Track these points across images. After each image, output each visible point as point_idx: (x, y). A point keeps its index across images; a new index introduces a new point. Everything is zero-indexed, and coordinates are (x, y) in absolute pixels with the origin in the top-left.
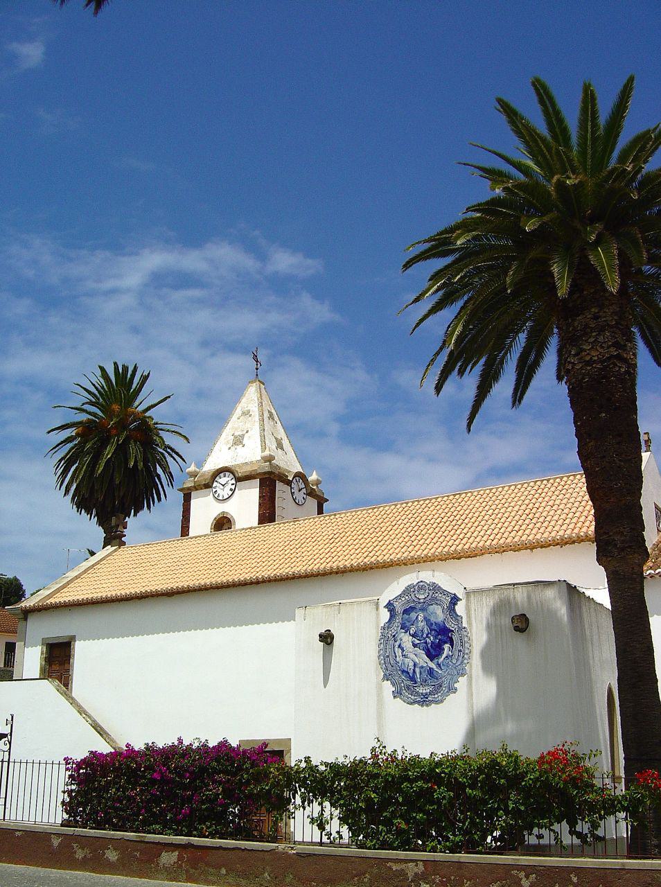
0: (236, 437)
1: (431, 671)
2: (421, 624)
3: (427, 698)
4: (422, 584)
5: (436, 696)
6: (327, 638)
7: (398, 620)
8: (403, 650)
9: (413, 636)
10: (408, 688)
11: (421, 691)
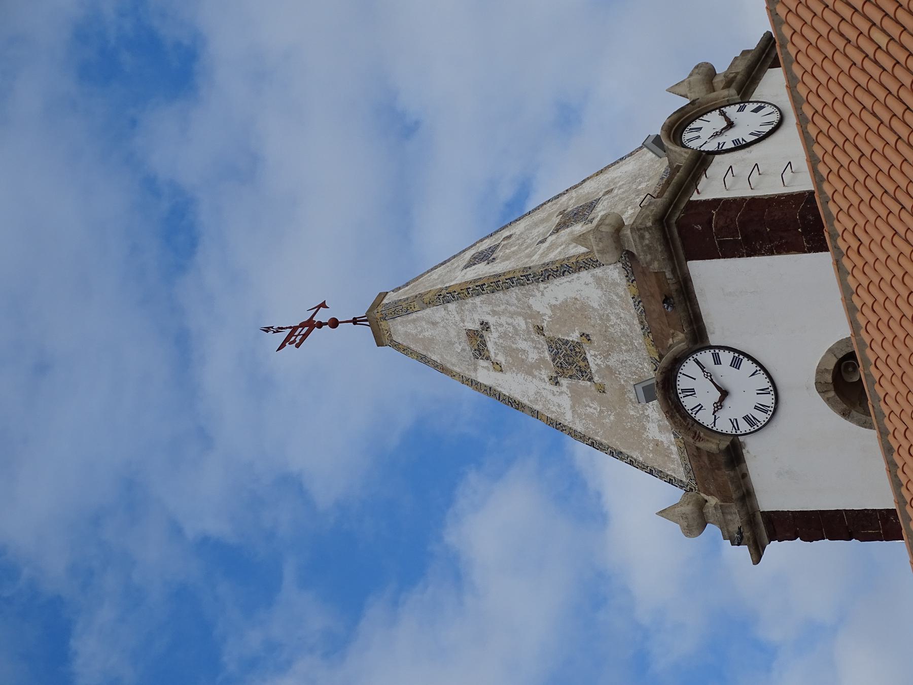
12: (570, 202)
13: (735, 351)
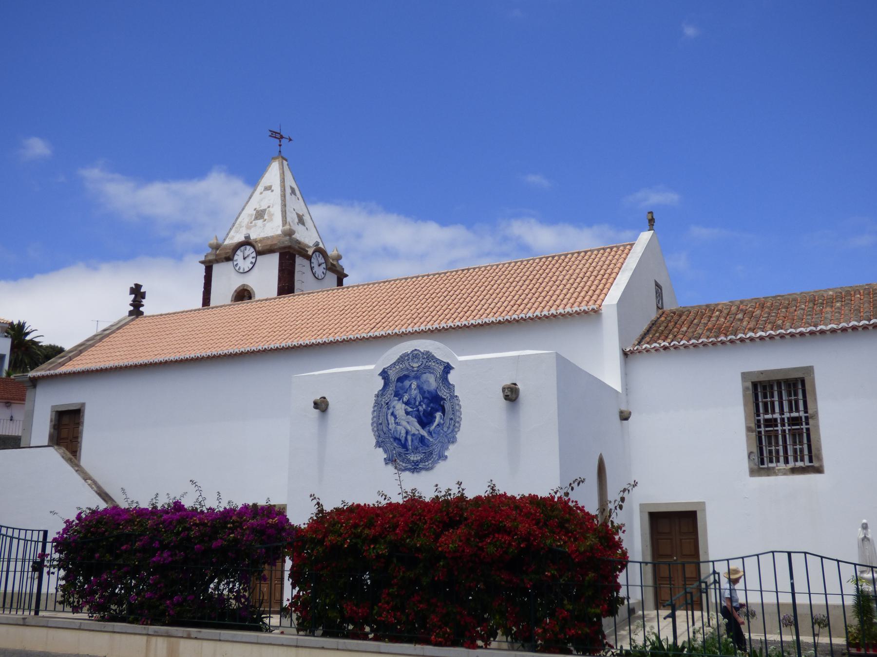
0: (258, 212)
1: (422, 439)
2: (414, 392)
3: (418, 465)
4: (416, 352)
5: (427, 463)
6: (321, 405)
7: (391, 389)
8: (395, 417)
9: (407, 403)
10: (400, 455)
11: (412, 459)
12: (307, 218)
13: (255, 263)
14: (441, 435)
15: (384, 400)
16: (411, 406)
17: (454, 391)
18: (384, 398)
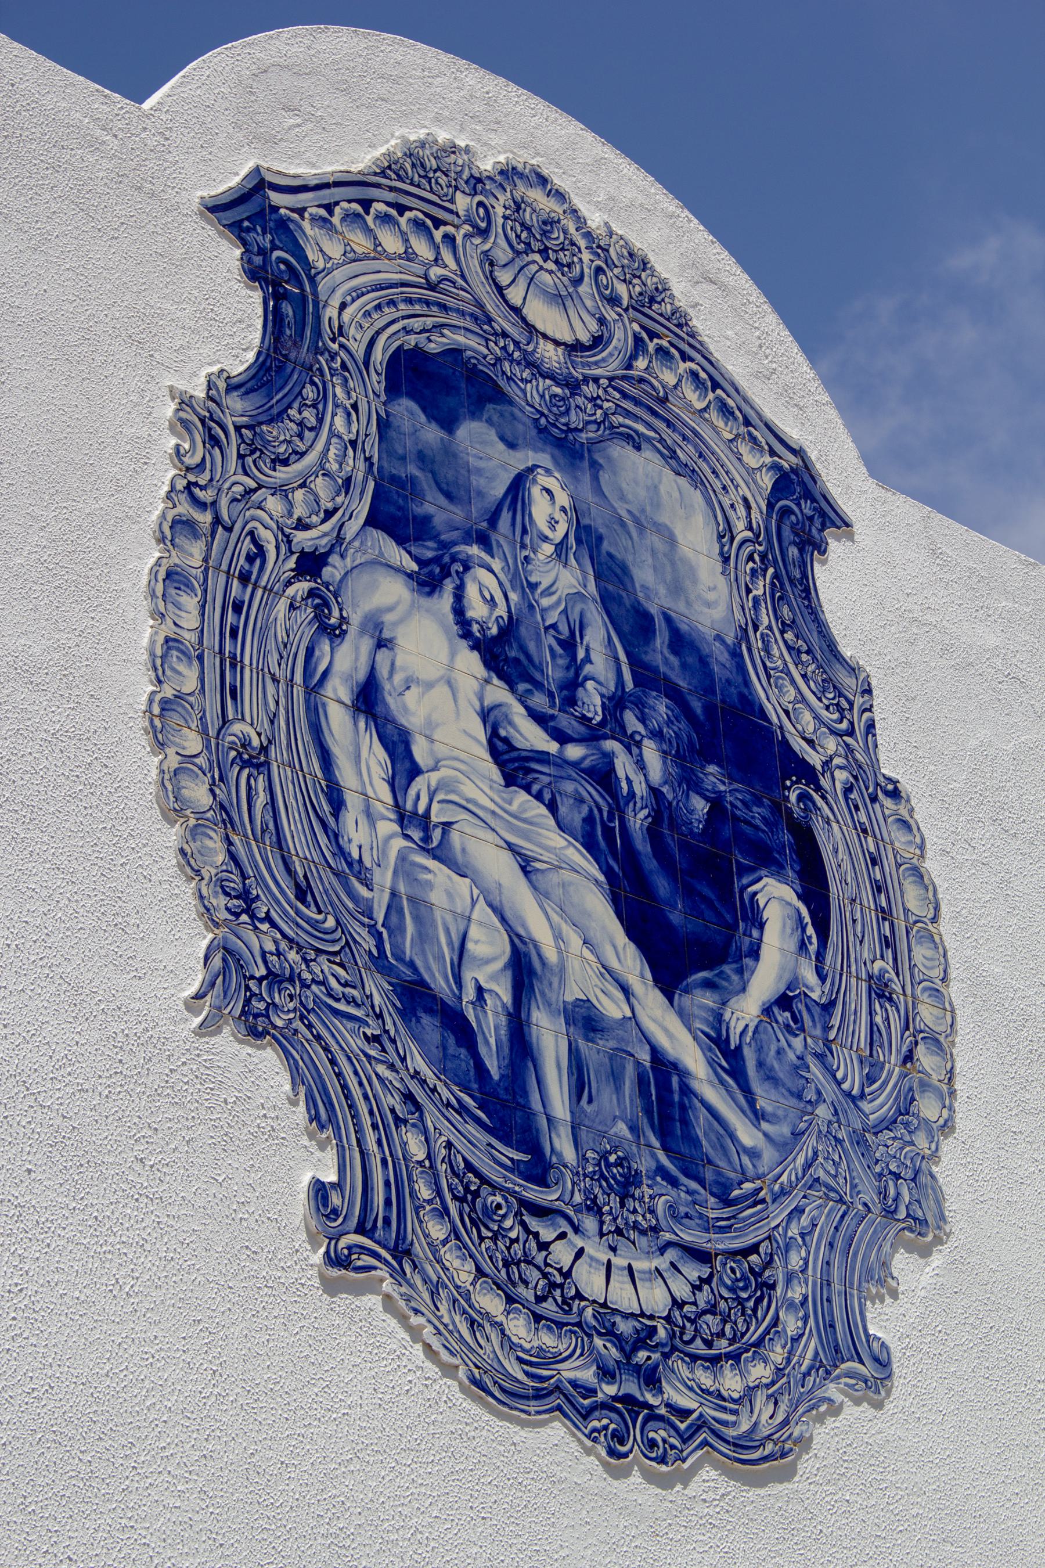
3: (651, 1379)
5: (731, 1383)
14: (823, 1111)
15: (274, 504)
16: (539, 701)
17: (871, 726)
18: (282, 491)
